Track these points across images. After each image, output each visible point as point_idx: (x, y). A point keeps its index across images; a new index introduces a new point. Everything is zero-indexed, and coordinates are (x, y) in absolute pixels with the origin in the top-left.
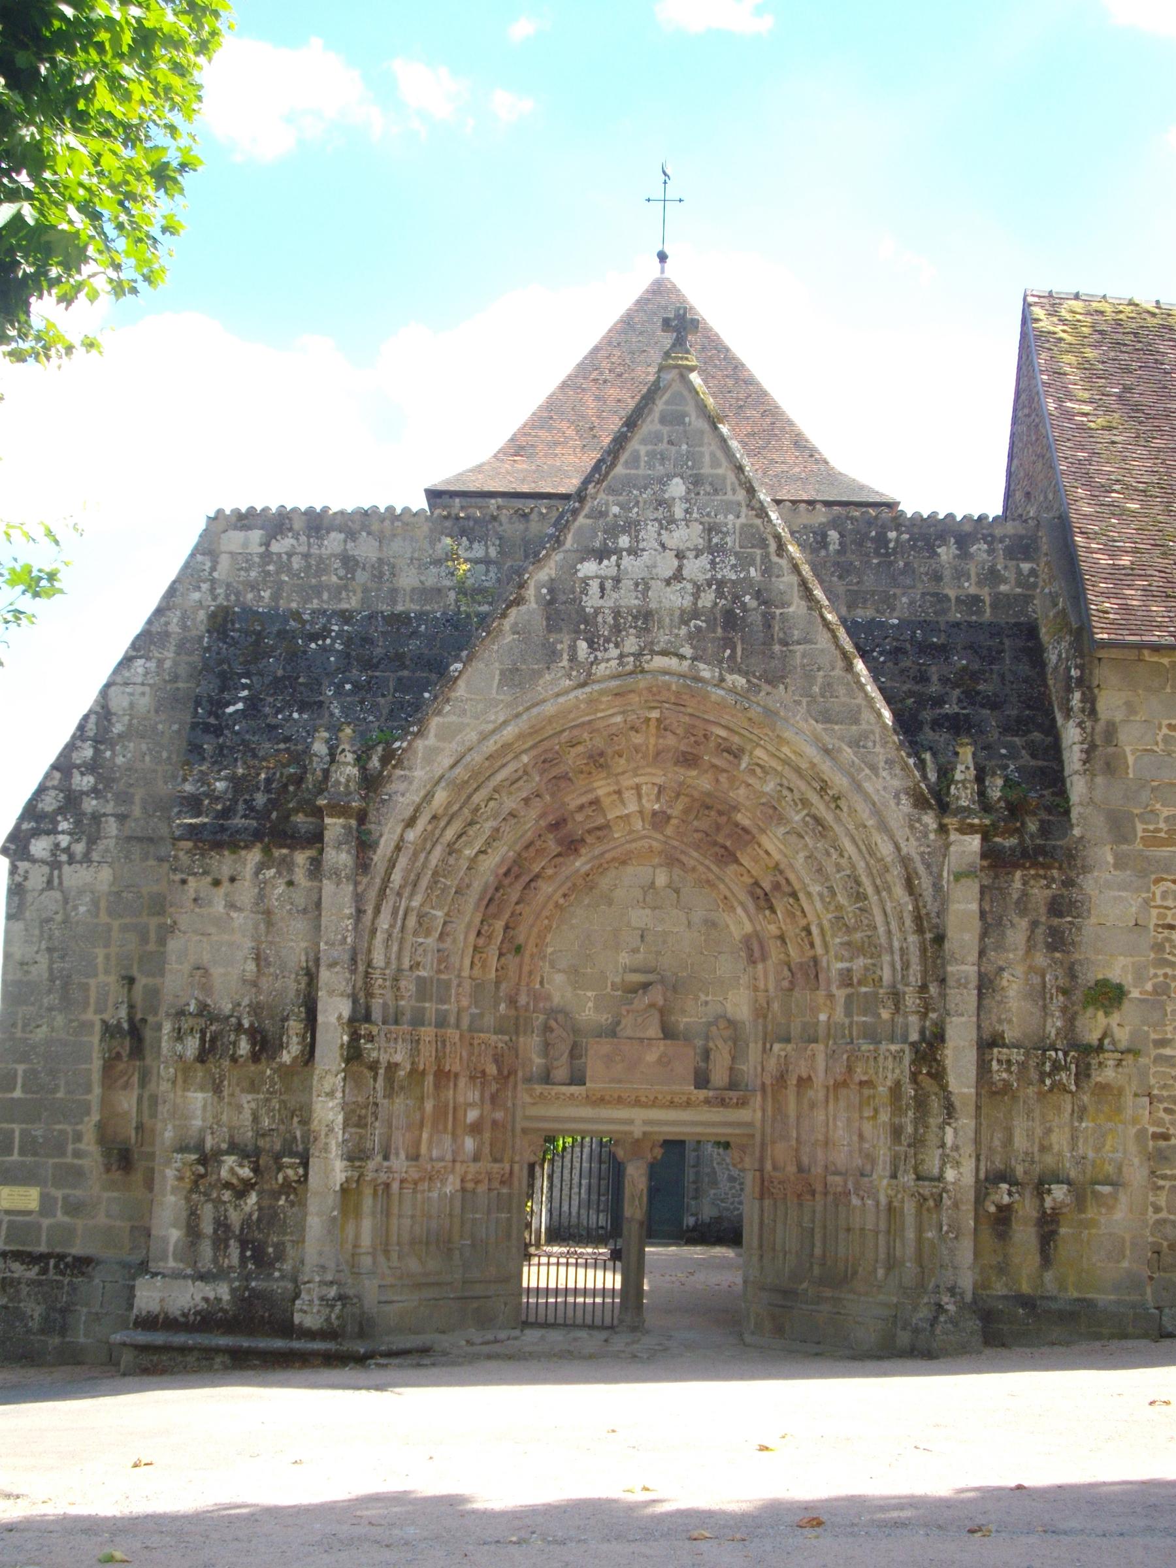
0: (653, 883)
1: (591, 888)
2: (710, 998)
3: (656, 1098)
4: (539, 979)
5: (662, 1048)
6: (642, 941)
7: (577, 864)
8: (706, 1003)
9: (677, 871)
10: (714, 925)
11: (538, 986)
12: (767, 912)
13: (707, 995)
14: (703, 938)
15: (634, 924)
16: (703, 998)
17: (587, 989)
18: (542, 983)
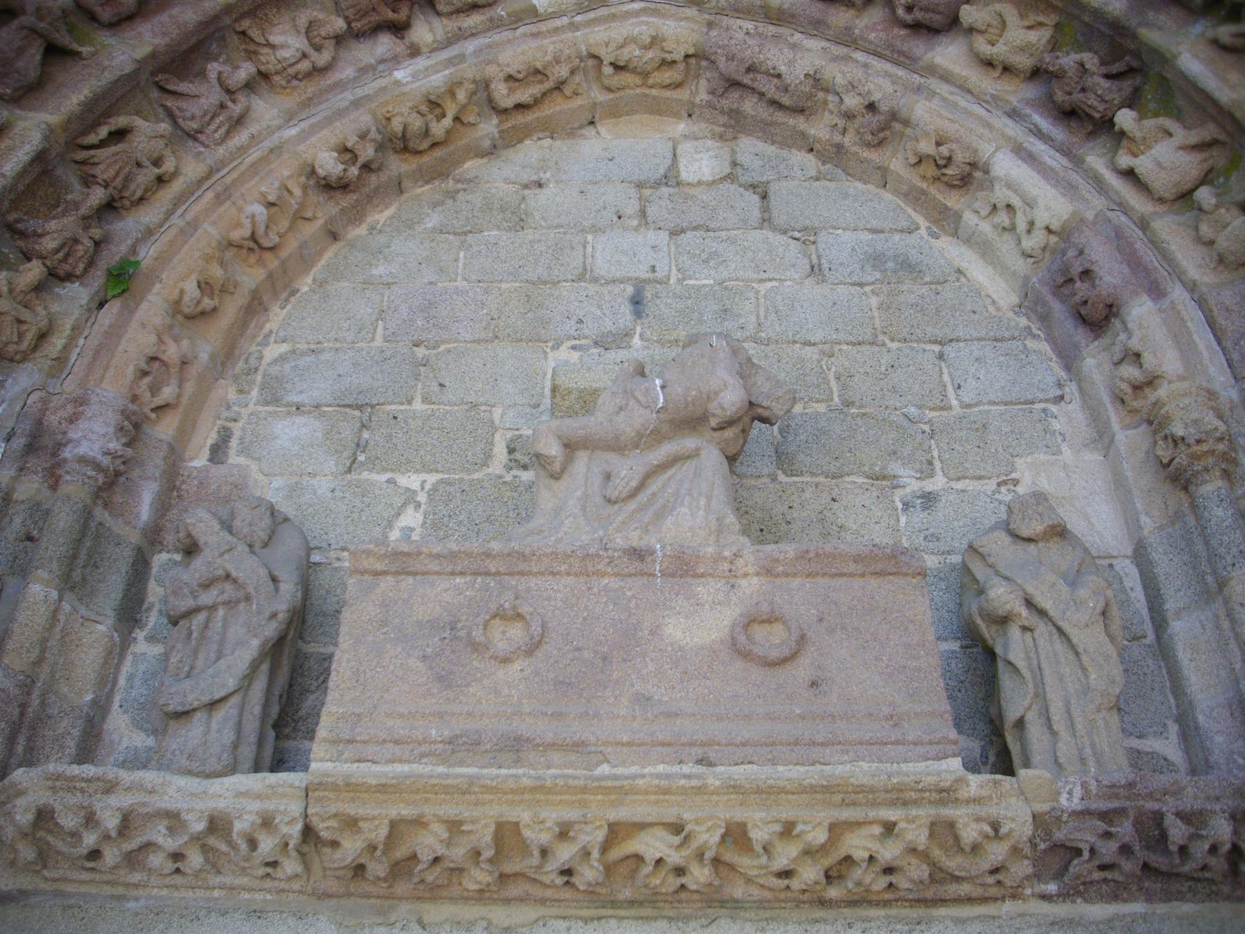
0: (670, 178)
1: (452, 195)
2: (938, 483)
3: (736, 835)
4: (213, 437)
5: (751, 586)
6: (638, 314)
7: (399, 75)
8: (929, 499)
9: (750, 148)
10: (908, 267)
11: (201, 461)
12: (1125, 118)
13: (927, 471)
14: (874, 301)
15: (602, 266)
16: (912, 485)
17: (404, 466)
18: (218, 452)
